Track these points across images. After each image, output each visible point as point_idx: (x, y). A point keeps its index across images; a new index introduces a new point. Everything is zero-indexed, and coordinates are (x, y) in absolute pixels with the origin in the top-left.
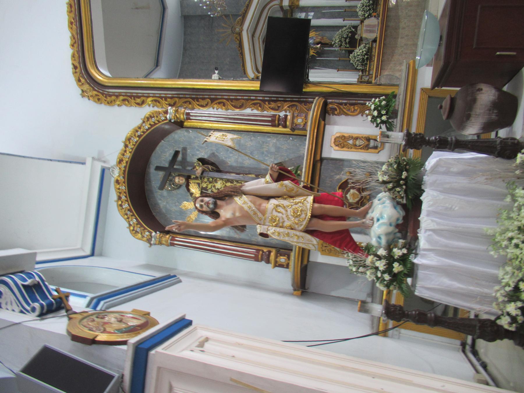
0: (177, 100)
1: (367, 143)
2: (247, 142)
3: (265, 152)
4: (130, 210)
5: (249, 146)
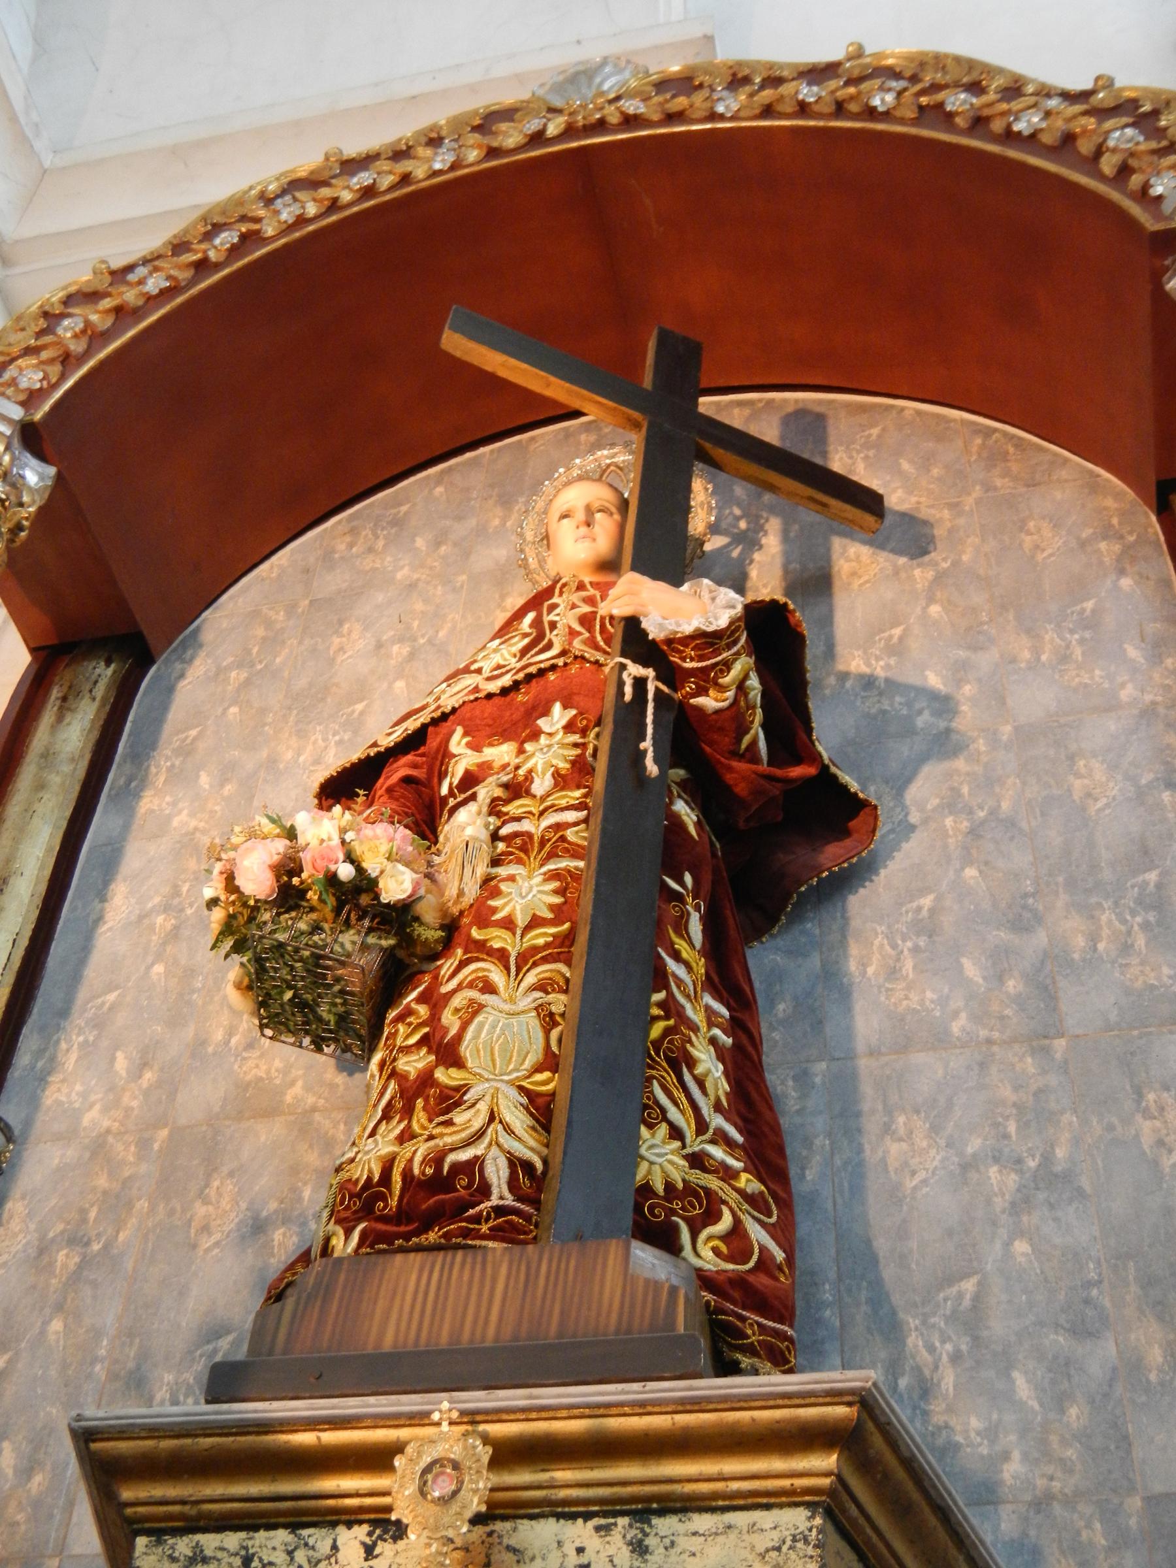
3: (1107, 1349)
4: (249, 239)
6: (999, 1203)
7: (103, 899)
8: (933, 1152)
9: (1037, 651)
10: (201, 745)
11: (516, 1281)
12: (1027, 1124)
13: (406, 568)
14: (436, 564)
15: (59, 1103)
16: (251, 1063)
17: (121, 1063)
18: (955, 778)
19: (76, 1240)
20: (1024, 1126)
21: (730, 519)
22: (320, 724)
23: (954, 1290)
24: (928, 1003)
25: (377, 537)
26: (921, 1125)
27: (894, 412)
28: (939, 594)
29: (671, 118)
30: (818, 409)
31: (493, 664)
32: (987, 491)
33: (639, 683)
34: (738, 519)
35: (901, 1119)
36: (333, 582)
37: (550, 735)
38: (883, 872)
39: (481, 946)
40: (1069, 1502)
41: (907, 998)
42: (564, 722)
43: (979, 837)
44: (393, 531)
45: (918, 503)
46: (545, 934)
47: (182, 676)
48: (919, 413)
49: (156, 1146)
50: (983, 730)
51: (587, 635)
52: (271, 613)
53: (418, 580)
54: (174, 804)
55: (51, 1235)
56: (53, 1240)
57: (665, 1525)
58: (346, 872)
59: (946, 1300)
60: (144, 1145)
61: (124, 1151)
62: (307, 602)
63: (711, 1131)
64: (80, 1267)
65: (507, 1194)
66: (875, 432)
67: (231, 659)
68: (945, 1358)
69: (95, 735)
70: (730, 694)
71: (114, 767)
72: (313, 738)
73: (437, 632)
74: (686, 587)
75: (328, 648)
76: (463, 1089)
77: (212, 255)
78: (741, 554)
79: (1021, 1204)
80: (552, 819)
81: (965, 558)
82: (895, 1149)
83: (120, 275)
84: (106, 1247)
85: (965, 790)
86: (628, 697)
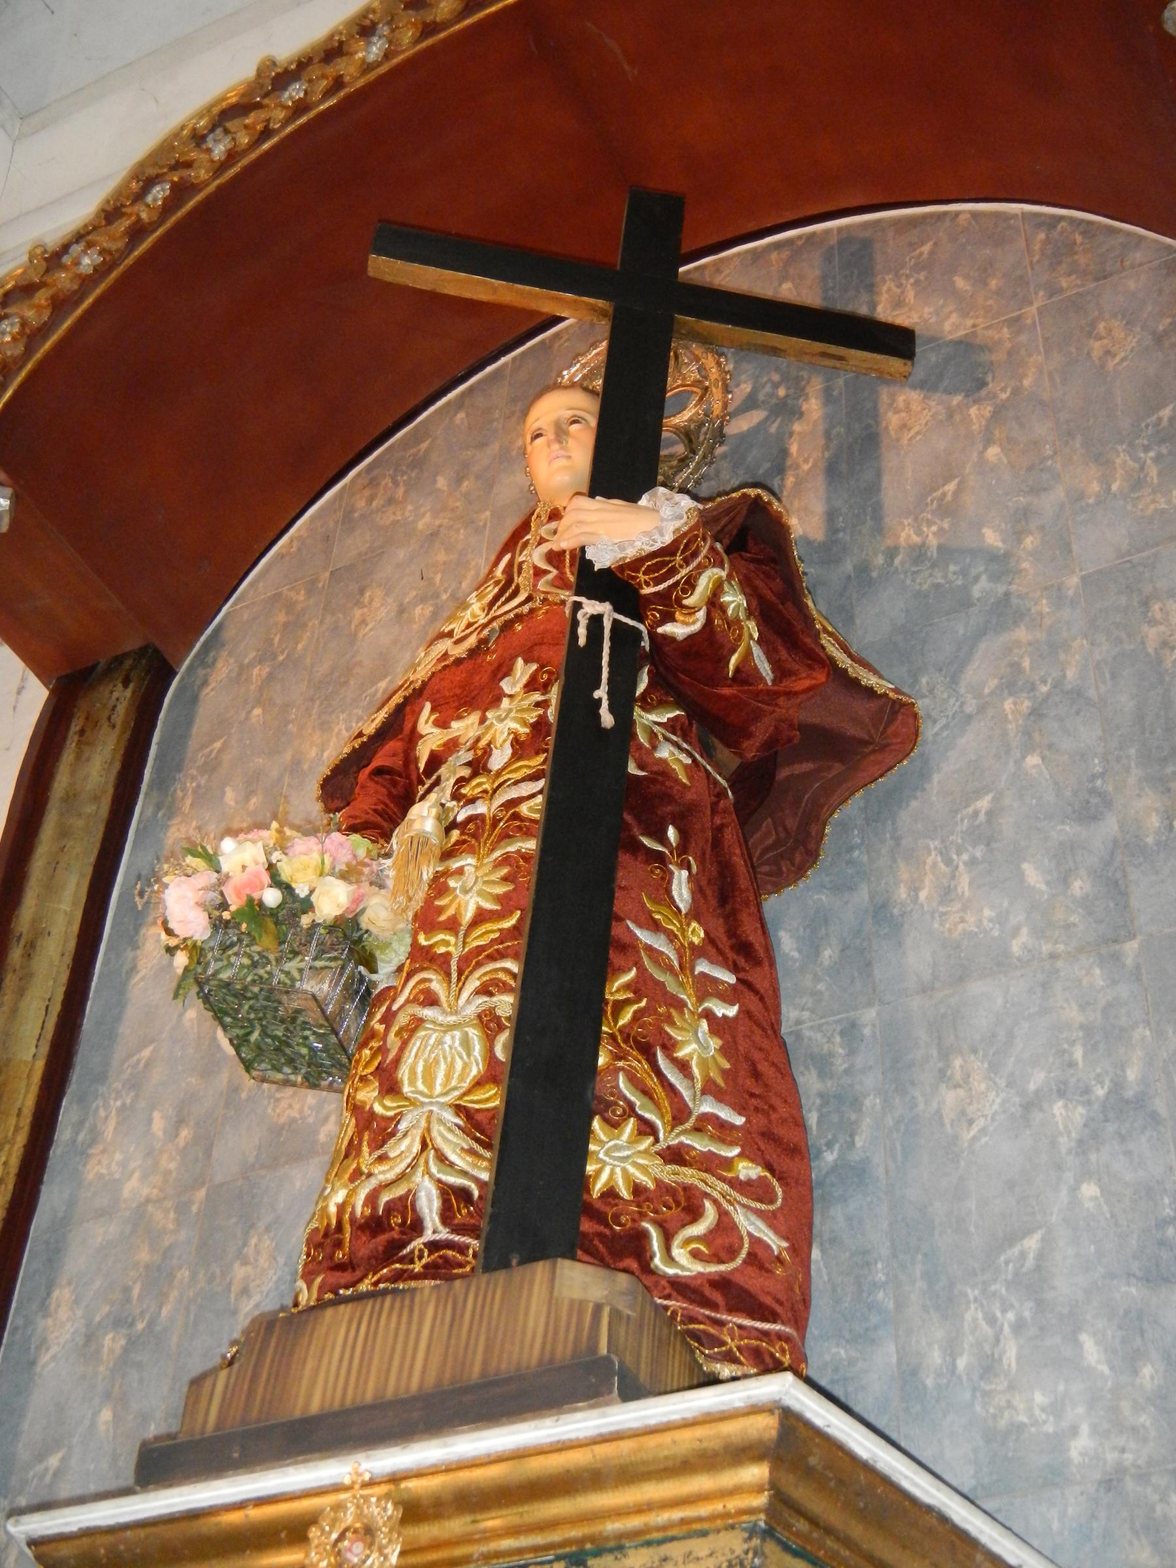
4: (181, 191)
6: (1064, 1143)
7: (136, 947)
8: (992, 1095)
9: (1106, 482)
10: (226, 758)
11: (442, 1323)
12: (1095, 1047)
13: (428, 515)
14: (458, 504)
15: (100, 1176)
16: (284, 1104)
17: (158, 1124)
18: (1016, 651)
19: (120, 1322)
20: (1091, 1050)
21: (768, 388)
22: (343, 712)
23: (1016, 1251)
24: (985, 922)
25: (396, 484)
26: (978, 1065)
27: (948, 220)
28: (997, 433)
30: (866, 234)
31: (463, 626)
32: (1051, 296)
34: (776, 386)
35: (958, 1063)
36: (355, 544)
37: (511, 696)
38: (936, 778)
40: (1143, 1477)
41: (963, 920)
42: (524, 680)
43: (1041, 716)
44: (413, 475)
45: (974, 326)
46: (492, 931)
47: (205, 683)
48: (975, 215)
49: (194, 1209)
50: (1046, 588)
51: (555, 572)
52: (292, 594)
53: (440, 526)
55: (97, 1319)
56: (100, 1323)
58: (272, 897)
59: (1007, 1263)
60: (182, 1209)
61: (163, 1218)
62: (327, 574)
63: (692, 1120)
64: (126, 1350)
65: (441, 1228)
66: (926, 248)
67: (252, 655)
68: (1006, 1328)
69: (117, 766)
70: (701, 615)
71: (141, 797)
72: (336, 730)
73: (460, 583)
74: (644, 501)
75: (350, 622)
76: (397, 1119)
77: (144, 216)
78: (779, 427)
79: (1089, 1139)
81: (1026, 383)
83: (54, 259)
84: (151, 1324)
85: (1026, 663)
86: (582, 641)
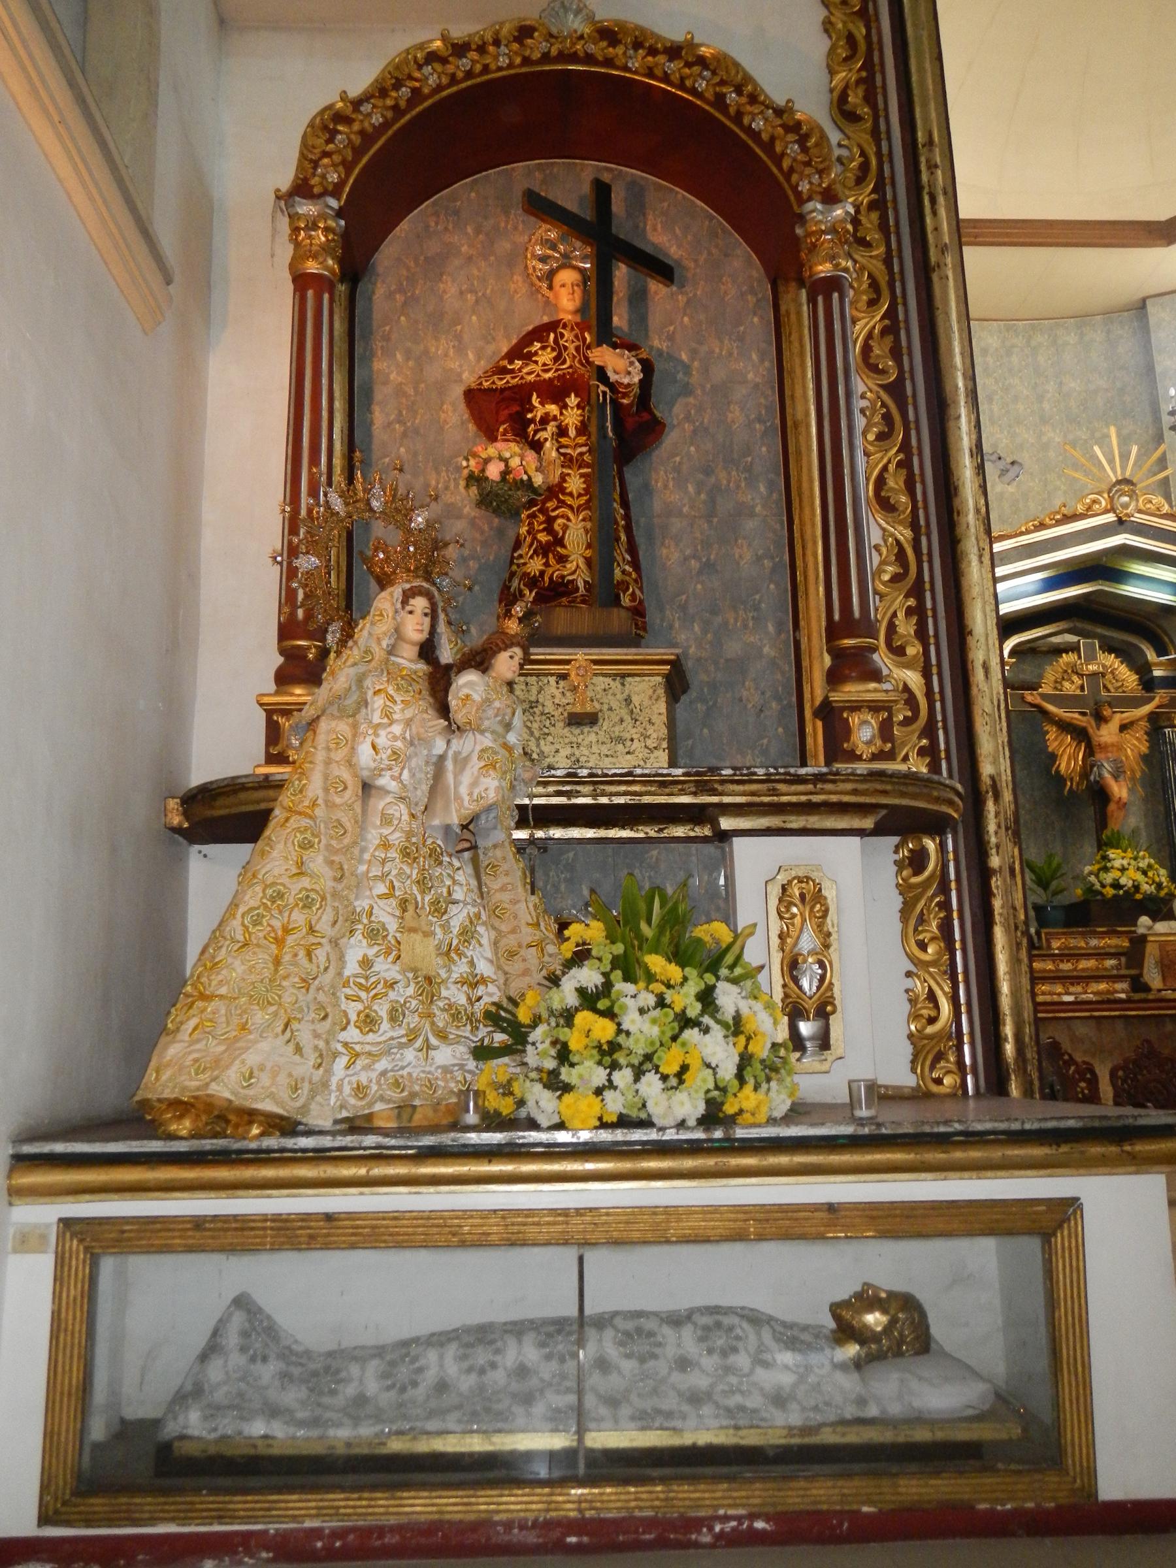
0: (880, 250)
1: (811, 1006)
2: (749, 545)
5: (737, 551)
6: (694, 572)
7: (371, 413)
26: (672, 543)
28: (688, 311)
29: (609, 62)
33: (604, 393)
36: (433, 247)
39: (563, 502)
40: (706, 660)
47: (373, 292)
54: (389, 367)
57: (629, 679)
58: (525, 477)
66: (666, 204)
76: (567, 557)
79: (700, 572)
80: (579, 450)
82: (665, 551)
85: (693, 412)
